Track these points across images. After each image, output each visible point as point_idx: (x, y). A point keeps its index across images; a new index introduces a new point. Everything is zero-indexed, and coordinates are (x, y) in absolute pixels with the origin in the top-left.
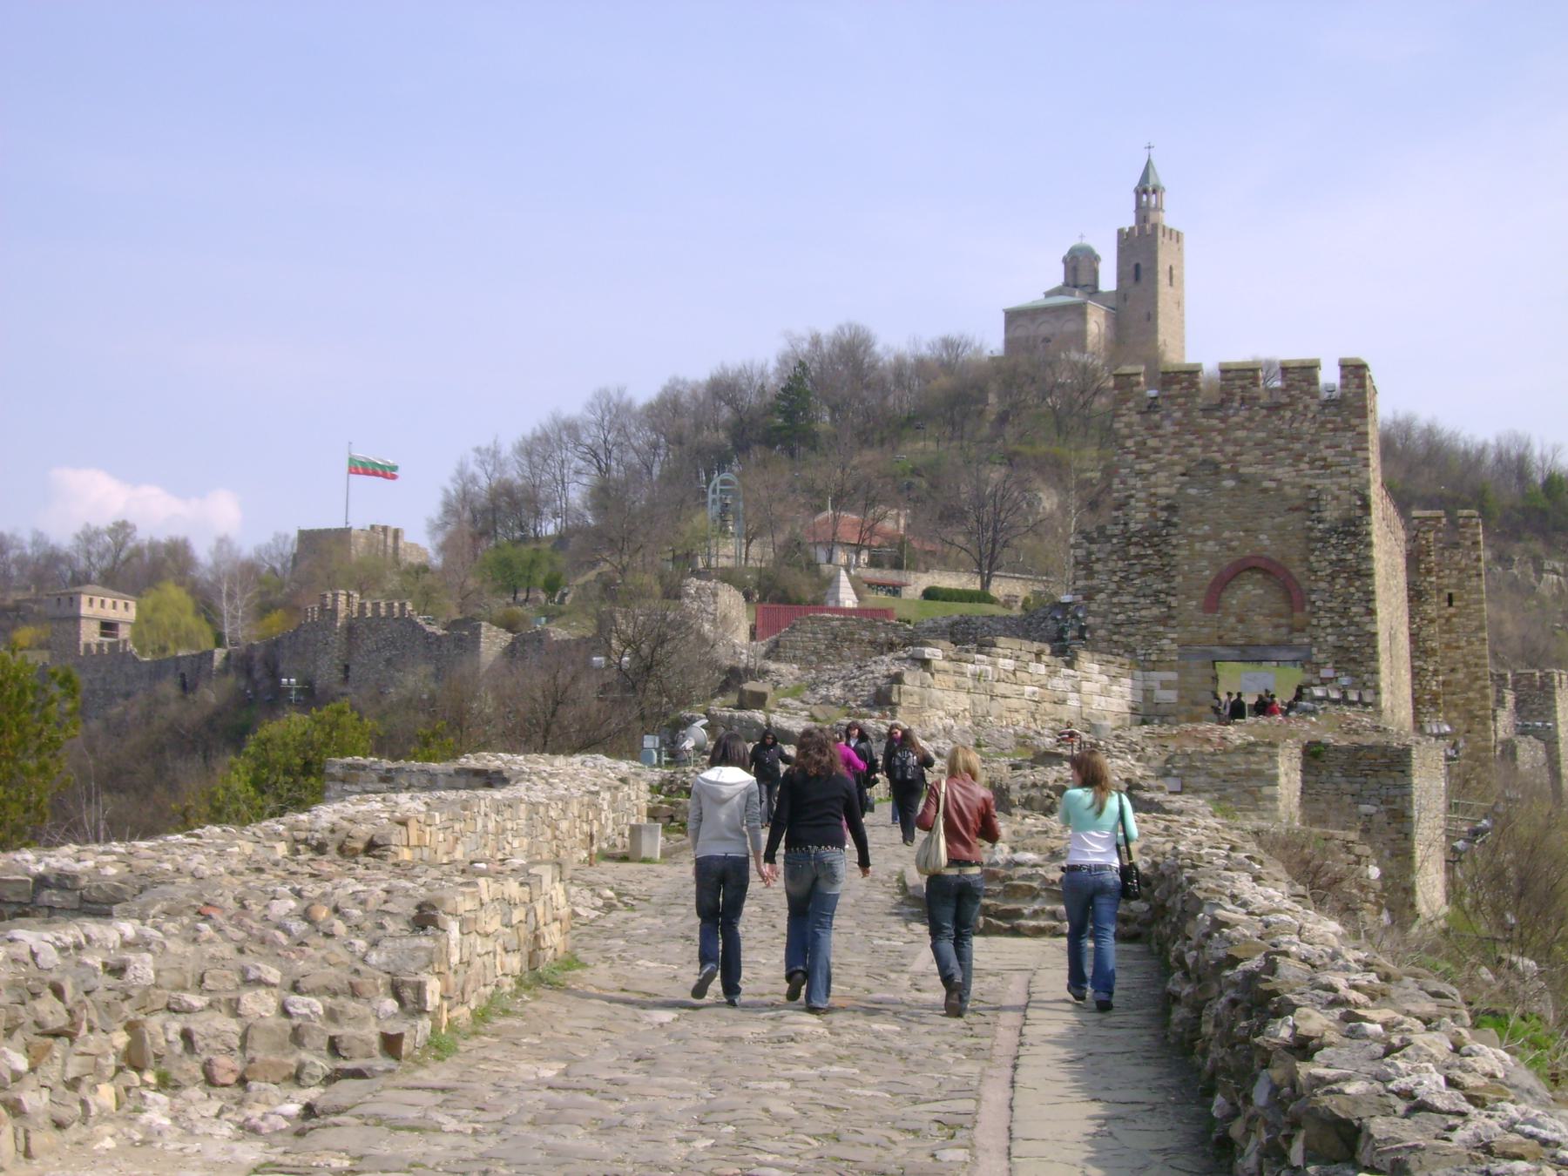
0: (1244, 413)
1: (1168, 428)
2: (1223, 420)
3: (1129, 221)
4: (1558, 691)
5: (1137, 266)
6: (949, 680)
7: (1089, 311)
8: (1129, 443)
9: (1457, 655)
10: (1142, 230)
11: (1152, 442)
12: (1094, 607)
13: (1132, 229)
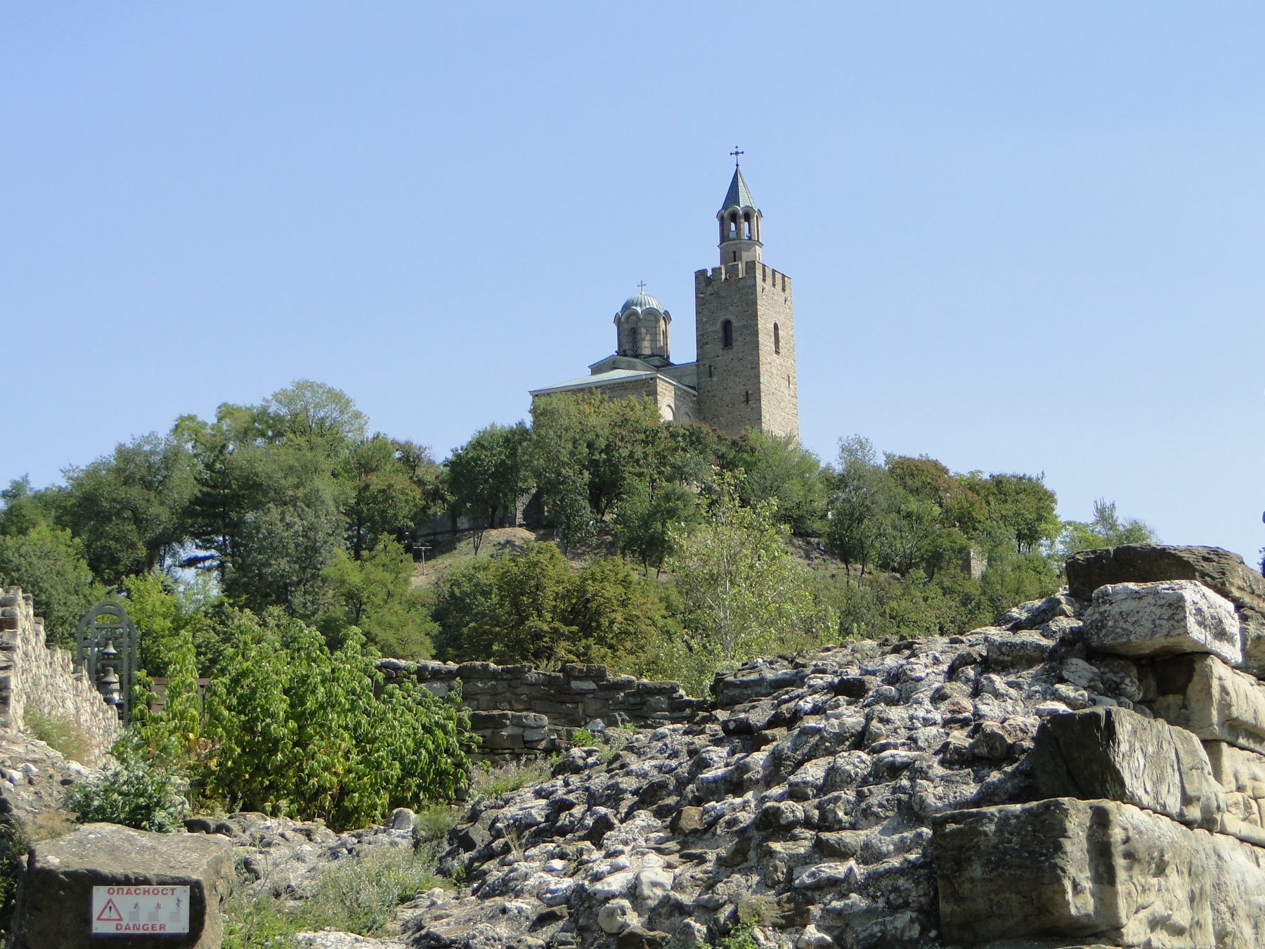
3: (711, 259)
5: (727, 325)
7: (659, 389)
10: (732, 271)
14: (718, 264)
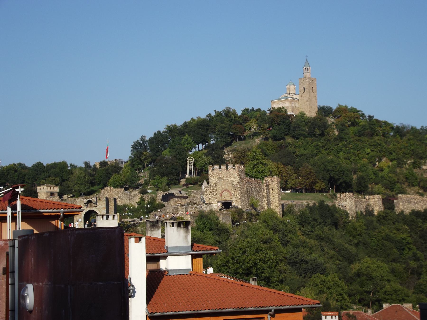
0: (224, 171)
1: (215, 173)
2: (221, 172)
8: (210, 175)
9: (273, 198)
11: (213, 175)
12: (207, 196)
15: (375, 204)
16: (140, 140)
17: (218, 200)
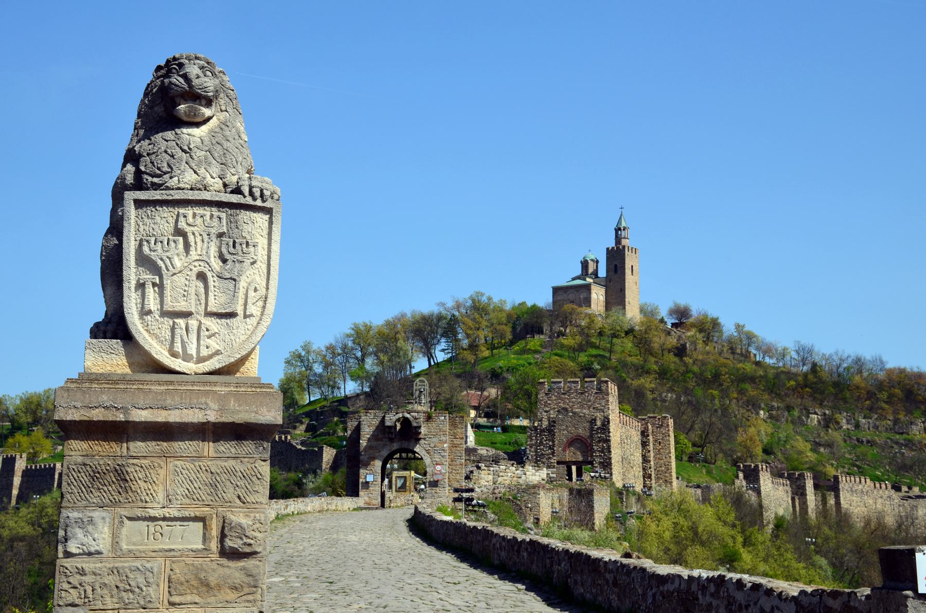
4: (761, 472)
5: (616, 266)
6: (486, 472)
9: (662, 462)
10: (618, 248)
13: (613, 248)
14: (613, 245)
15: (801, 491)
16: (300, 350)
17: (559, 459)
